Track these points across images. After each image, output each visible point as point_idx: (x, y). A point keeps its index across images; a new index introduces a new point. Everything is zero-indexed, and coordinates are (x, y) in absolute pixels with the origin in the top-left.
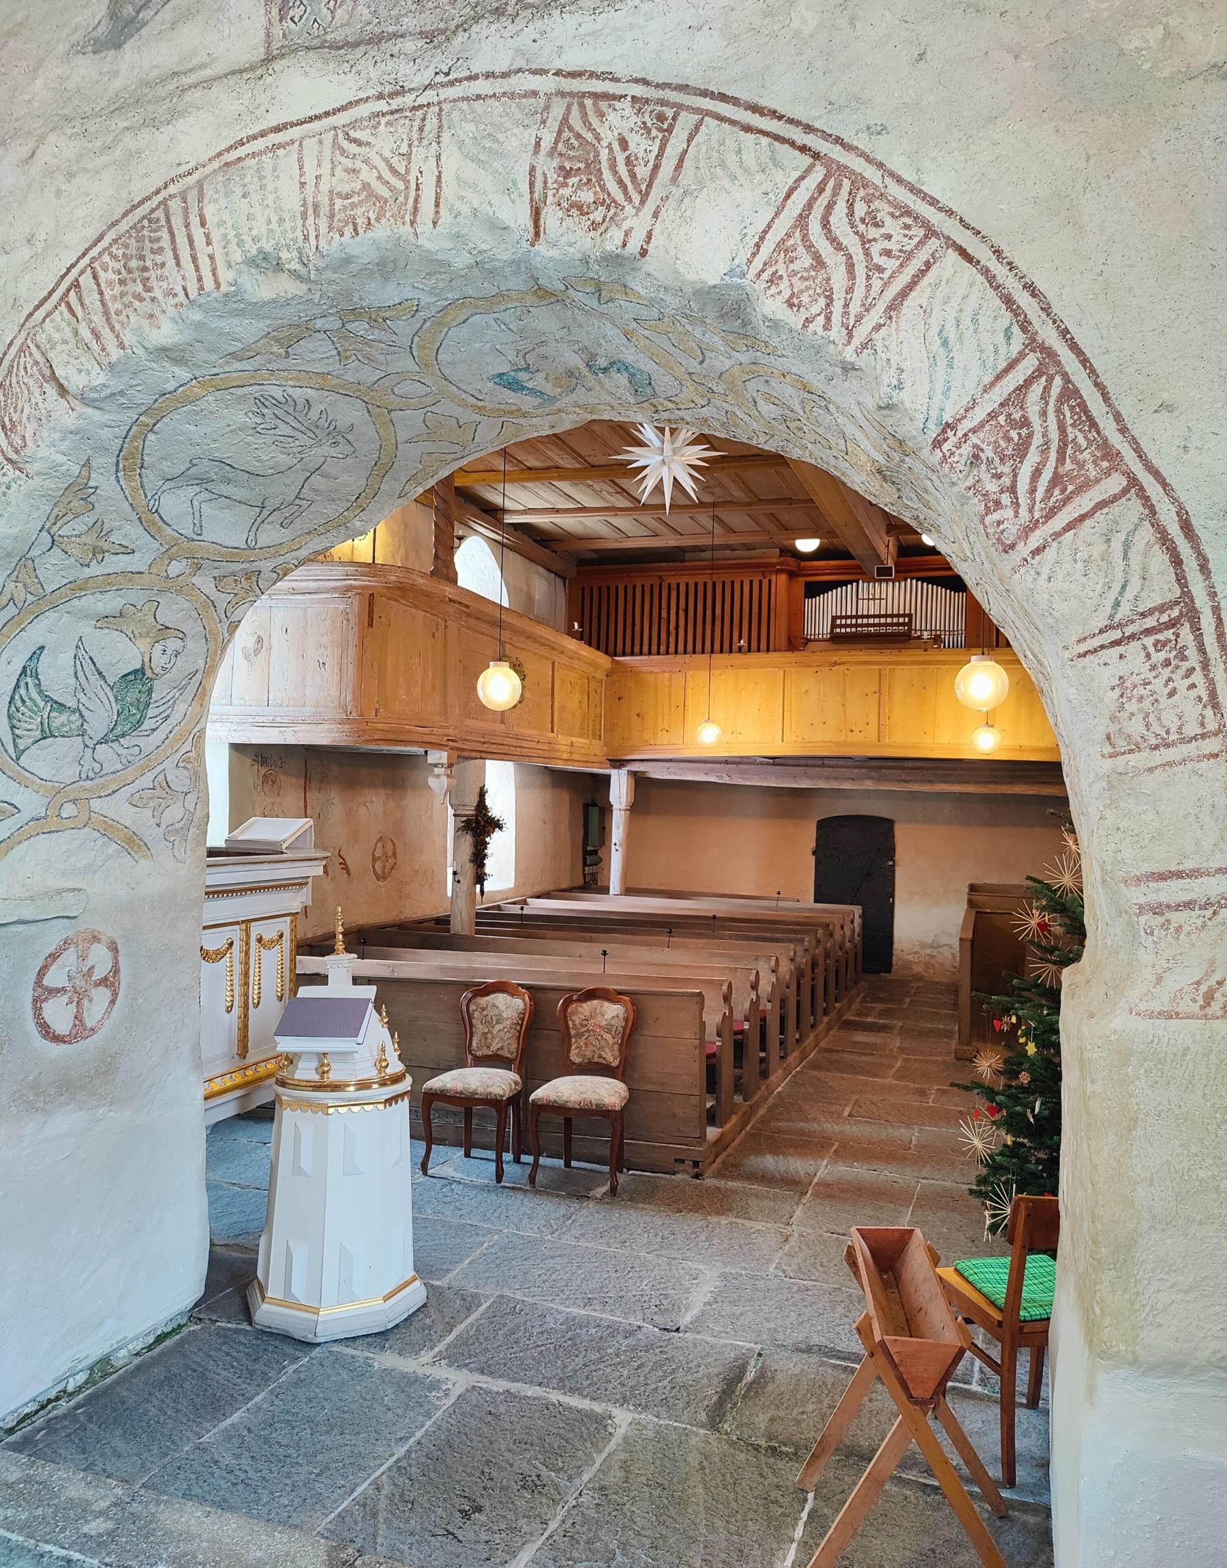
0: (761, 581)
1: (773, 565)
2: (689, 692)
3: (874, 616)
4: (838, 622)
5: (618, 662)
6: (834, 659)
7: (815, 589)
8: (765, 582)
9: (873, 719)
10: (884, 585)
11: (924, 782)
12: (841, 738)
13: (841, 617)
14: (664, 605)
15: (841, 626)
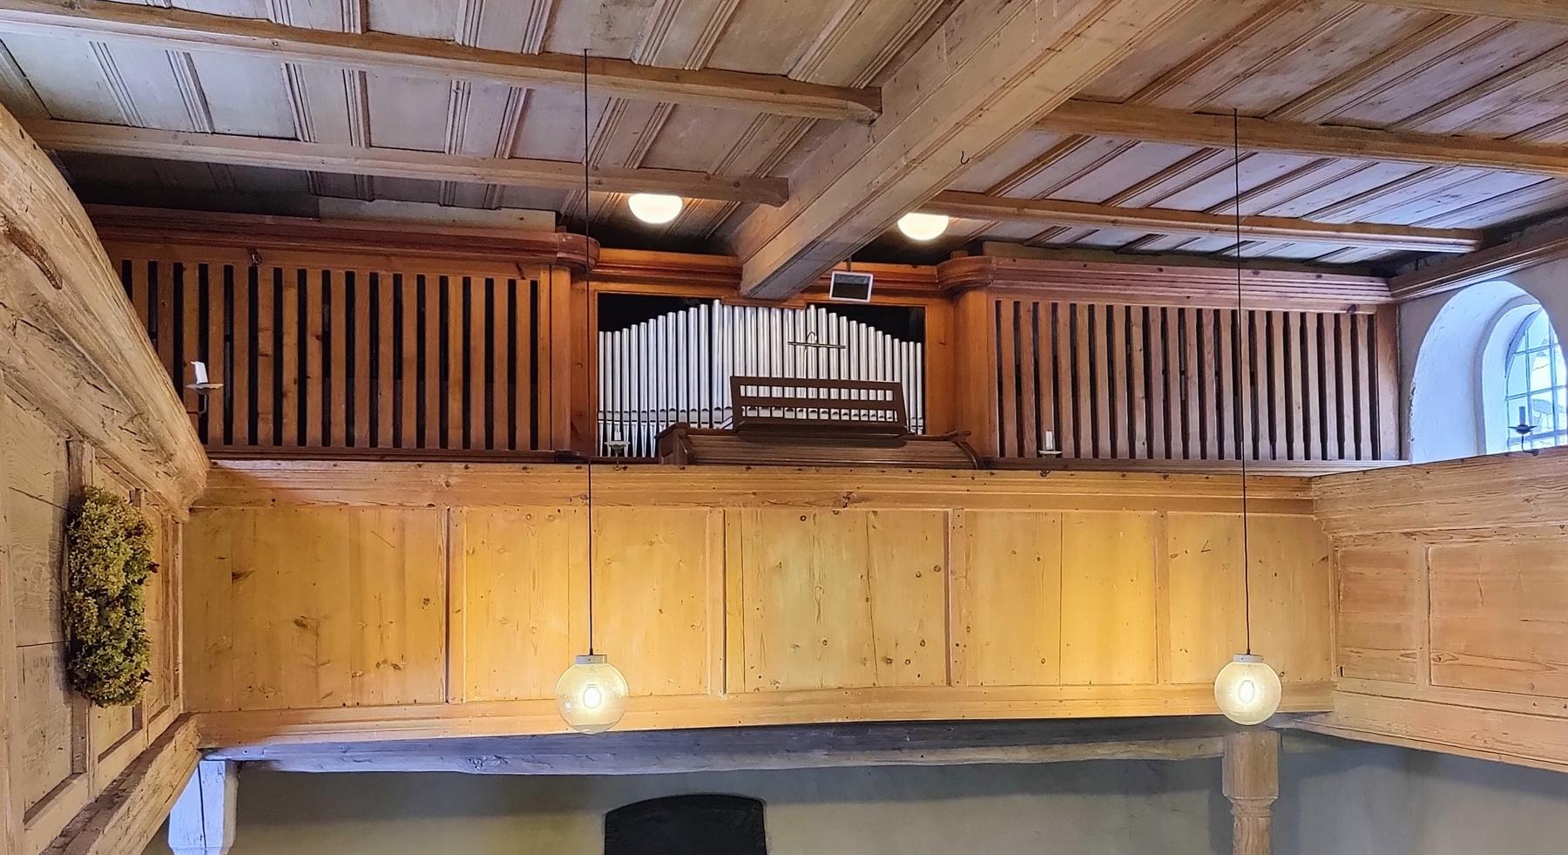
0: (512, 285)
1: (549, 248)
2: (462, 564)
3: (807, 383)
4: (751, 391)
5: (230, 475)
6: (846, 488)
7: (620, 313)
8: (523, 289)
9: (935, 632)
10: (763, 313)
11: (931, 748)
12: (860, 677)
13: (758, 381)
14: (265, 319)
15: (756, 402)
